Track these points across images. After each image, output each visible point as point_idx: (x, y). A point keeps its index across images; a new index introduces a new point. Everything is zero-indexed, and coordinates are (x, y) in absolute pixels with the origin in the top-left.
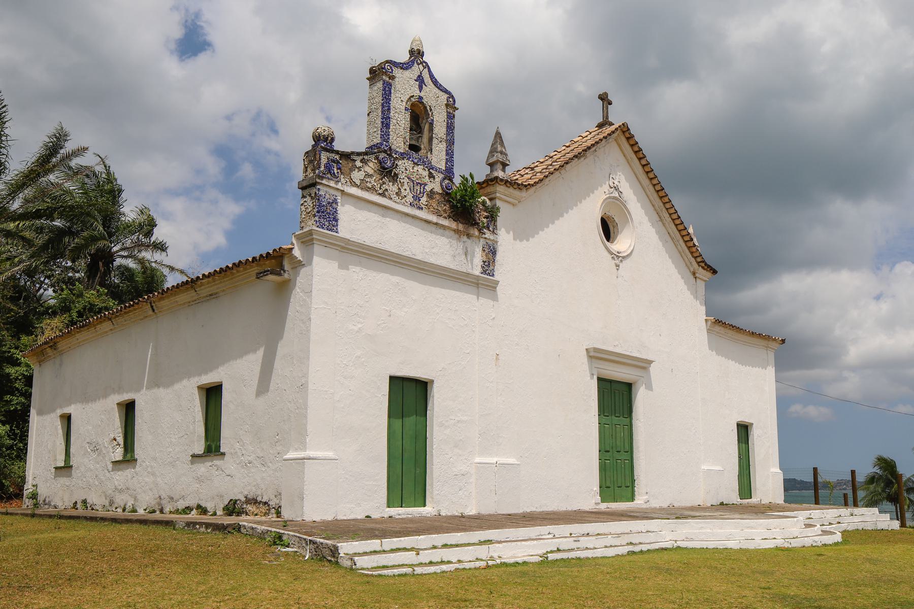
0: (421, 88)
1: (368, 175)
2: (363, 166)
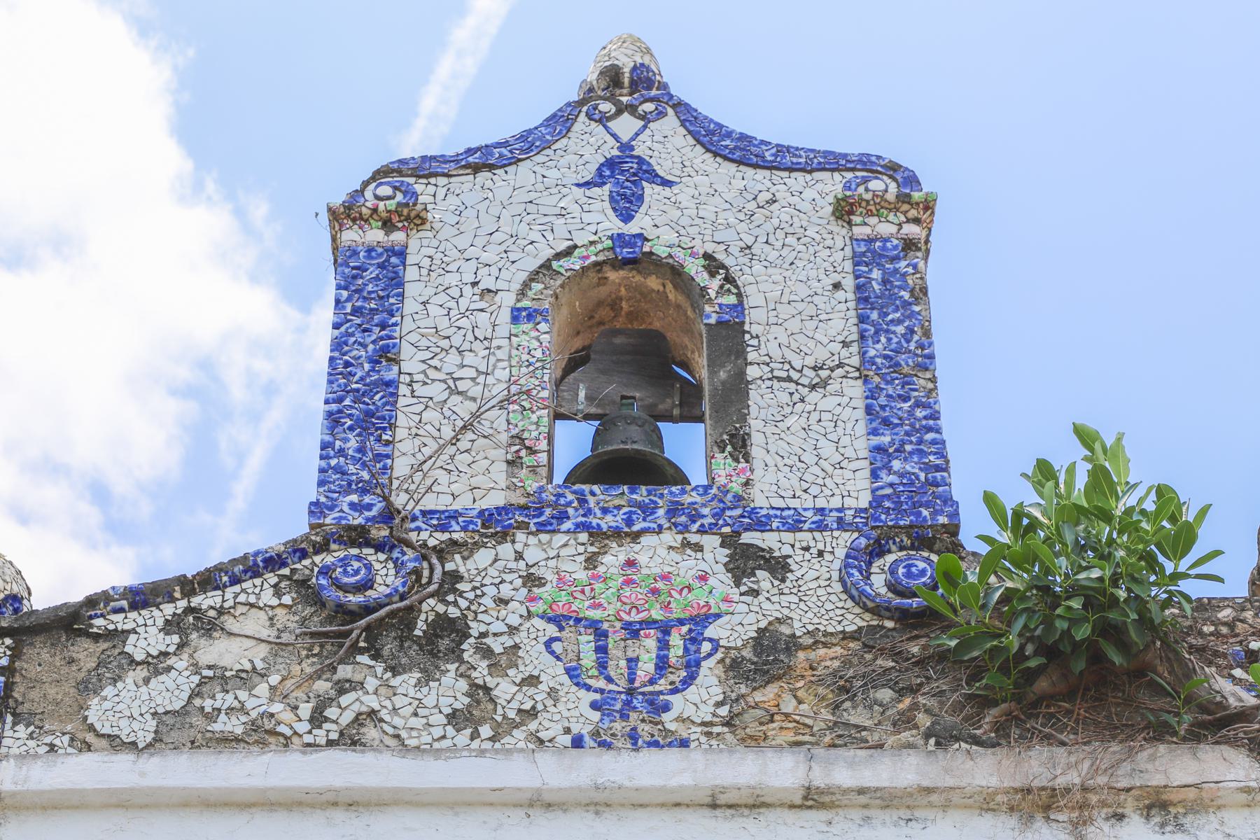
0: (626, 206)
1: (220, 678)
2: (181, 646)
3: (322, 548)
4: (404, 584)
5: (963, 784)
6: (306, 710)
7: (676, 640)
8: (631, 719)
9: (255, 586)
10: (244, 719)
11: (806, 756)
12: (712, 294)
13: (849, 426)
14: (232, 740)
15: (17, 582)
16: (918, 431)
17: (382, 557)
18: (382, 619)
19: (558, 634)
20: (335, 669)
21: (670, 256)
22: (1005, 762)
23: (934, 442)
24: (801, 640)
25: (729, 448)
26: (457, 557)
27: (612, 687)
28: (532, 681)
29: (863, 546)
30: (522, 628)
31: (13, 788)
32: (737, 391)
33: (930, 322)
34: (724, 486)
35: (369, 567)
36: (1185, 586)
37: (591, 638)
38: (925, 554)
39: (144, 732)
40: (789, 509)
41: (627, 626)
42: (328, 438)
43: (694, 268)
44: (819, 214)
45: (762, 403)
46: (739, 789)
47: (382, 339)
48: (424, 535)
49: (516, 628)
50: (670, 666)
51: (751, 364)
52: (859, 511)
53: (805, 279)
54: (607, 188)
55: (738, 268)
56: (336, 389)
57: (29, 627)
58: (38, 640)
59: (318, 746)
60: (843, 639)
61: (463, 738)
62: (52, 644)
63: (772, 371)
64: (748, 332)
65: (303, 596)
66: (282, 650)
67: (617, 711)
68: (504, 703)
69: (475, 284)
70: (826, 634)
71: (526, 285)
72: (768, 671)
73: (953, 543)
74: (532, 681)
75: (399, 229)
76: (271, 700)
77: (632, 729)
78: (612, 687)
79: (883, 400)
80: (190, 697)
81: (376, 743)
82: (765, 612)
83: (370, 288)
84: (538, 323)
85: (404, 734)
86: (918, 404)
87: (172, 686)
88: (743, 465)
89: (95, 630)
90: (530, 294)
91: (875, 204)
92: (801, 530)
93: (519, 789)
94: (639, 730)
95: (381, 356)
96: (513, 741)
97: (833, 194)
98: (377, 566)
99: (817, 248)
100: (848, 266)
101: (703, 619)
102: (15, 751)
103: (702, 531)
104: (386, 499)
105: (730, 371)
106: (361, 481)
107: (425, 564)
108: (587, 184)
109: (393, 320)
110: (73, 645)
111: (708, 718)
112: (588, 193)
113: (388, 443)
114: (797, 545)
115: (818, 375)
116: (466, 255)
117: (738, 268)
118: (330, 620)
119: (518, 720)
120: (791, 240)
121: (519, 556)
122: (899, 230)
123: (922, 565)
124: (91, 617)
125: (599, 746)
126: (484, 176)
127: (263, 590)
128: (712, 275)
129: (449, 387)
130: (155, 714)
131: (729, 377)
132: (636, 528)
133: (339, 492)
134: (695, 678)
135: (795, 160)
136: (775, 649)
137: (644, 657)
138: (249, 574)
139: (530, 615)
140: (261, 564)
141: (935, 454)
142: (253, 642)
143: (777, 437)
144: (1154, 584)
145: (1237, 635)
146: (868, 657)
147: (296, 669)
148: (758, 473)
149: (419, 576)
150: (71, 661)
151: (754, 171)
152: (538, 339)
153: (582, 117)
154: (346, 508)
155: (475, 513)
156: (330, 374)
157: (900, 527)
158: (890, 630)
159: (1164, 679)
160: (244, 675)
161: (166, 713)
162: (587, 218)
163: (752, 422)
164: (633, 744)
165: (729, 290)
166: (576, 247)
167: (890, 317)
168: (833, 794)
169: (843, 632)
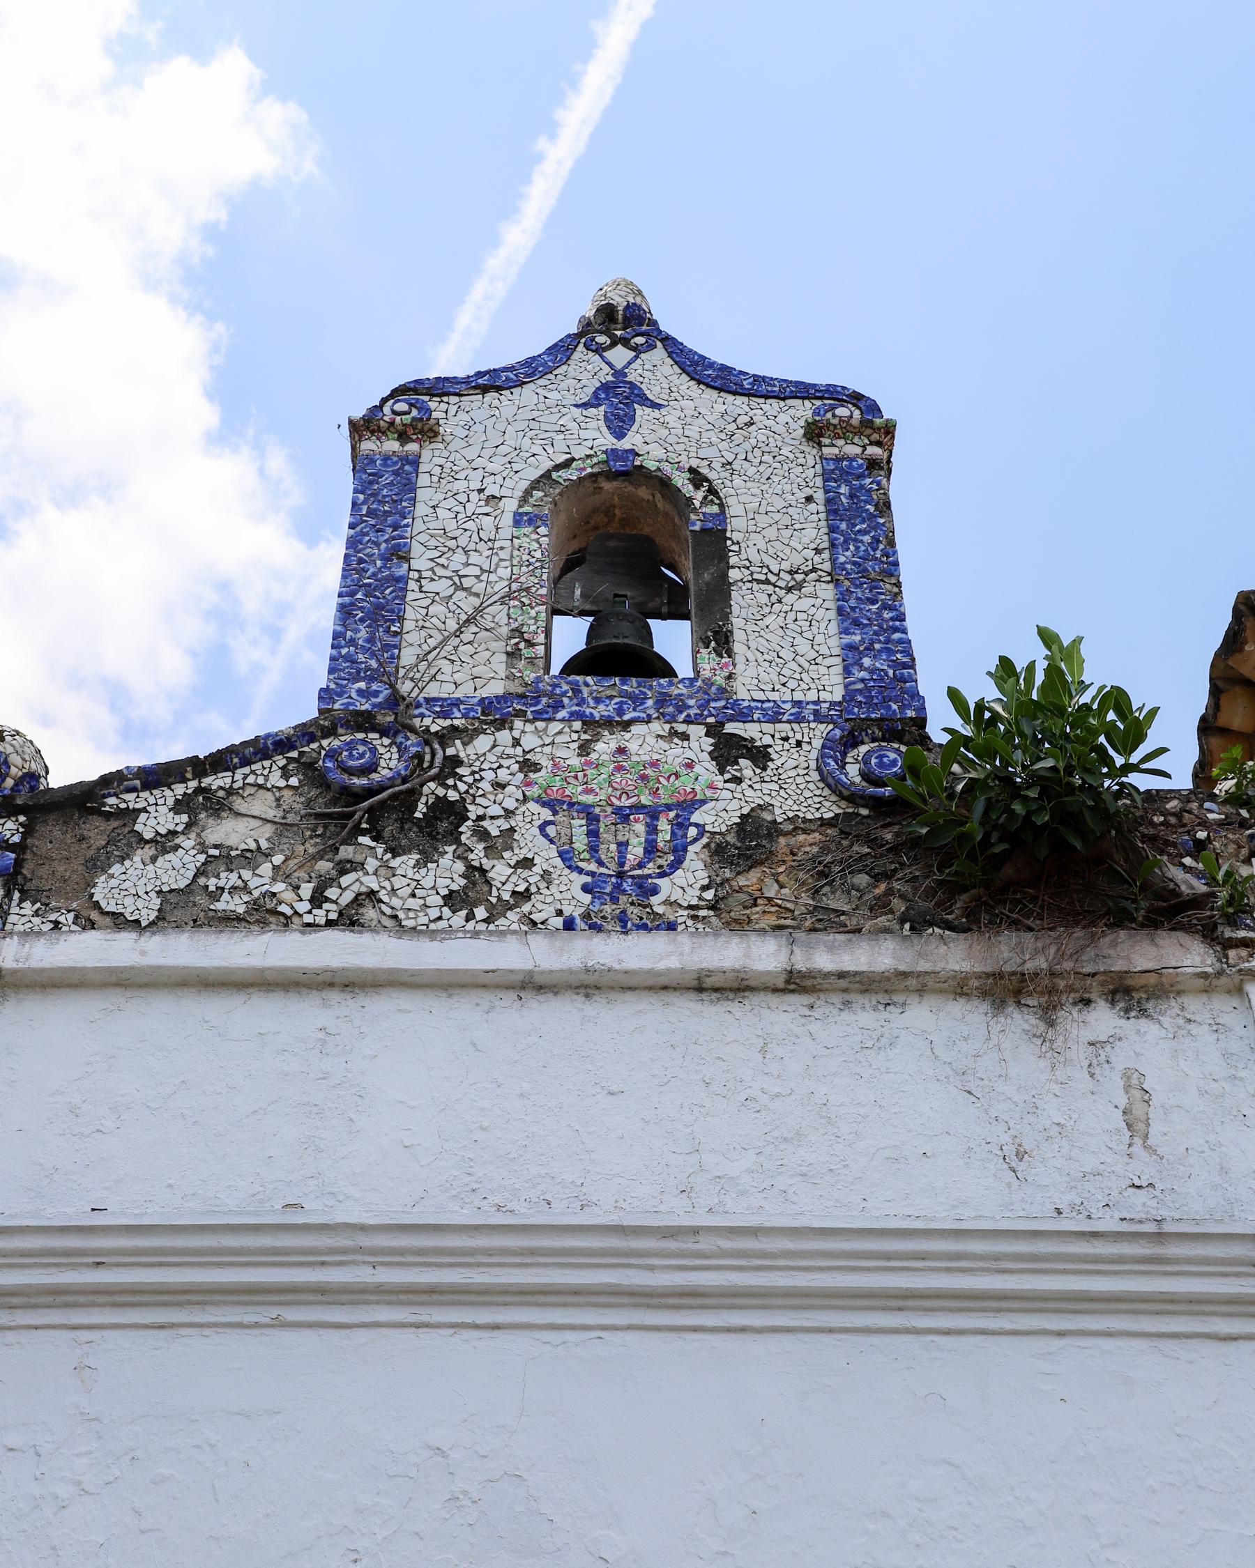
0: (619, 424)
1: (227, 858)
2: (189, 826)
3: (330, 732)
4: (406, 768)
5: (937, 969)
6: (307, 890)
7: (664, 825)
8: (621, 902)
9: (264, 768)
10: (246, 898)
11: (788, 940)
12: (697, 504)
13: (823, 625)
14: (233, 919)
15: (35, 761)
16: (885, 631)
17: (386, 741)
18: (383, 802)
19: (552, 818)
20: (337, 849)
21: (659, 469)
22: (976, 947)
23: (900, 641)
24: (782, 826)
25: (713, 644)
26: (458, 742)
27: (603, 870)
28: (527, 863)
29: (838, 737)
30: (517, 812)
31: (13, 965)
32: (720, 592)
33: (893, 532)
34: (709, 679)
35: (374, 750)
36: (1134, 779)
37: (584, 822)
38: (896, 746)
39: (147, 910)
40: (769, 701)
41: (618, 811)
42: (339, 628)
43: (681, 481)
44: (791, 436)
45: (743, 604)
46: (724, 972)
47: (394, 538)
48: (427, 721)
49: (512, 812)
50: (658, 850)
51: (733, 567)
52: (833, 704)
53: (780, 493)
54: (602, 408)
55: (720, 481)
56: (349, 583)
57: (43, 805)
58: (51, 818)
59: (318, 926)
60: (821, 825)
61: (459, 919)
62: (64, 822)
63: (752, 574)
64: (730, 539)
65: (309, 778)
66: (287, 830)
67: (607, 894)
68: (499, 885)
69: (481, 491)
70: (805, 820)
71: (528, 493)
72: (751, 856)
73: (920, 735)
74: (527, 863)
75: (413, 441)
76: (274, 879)
77: (621, 912)
78: (603, 870)
79: (853, 603)
80: (195, 876)
81: (374, 923)
82: (748, 799)
83: (385, 492)
84: (539, 527)
85: (401, 915)
86: (885, 607)
87: (178, 864)
88: (726, 660)
89: (107, 809)
90: (531, 500)
91: (842, 428)
92: (780, 722)
93: (512, 971)
94: (629, 912)
95: (392, 554)
96: (507, 923)
97: (804, 418)
98: (382, 750)
99: (791, 465)
100: (819, 481)
101: (690, 804)
102: (19, 928)
103: (688, 721)
104: (392, 686)
105: (713, 574)
106: (370, 669)
107: (427, 749)
108: (585, 405)
109: (405, 522)
110: (84, 823)
111: (695, 902)
112: (585, 413)
113: (396, 634)
114: (777, 736)
115: (793, 579)
116: (474, 465)
117: (720, 481)
118: (334, 802)
119: (512, 902)
120: (767, 458)
121: (516, 742)
122: (864, 451)
123: (892, 756)
124: (104, 796)
125: (590, 929)
126: (491, 396)
127: (272, 772)
128: (697, 487)
129: (455, 583)
130: (159, 893)
131: (713, 578)
132: (626, 717)
133: (348, 680)
134: (682, 862)
135: (770, 389)
136: (758, 834)
137: (634, 841)
138: (259, 756)
139: (525, 799)
140: (271, 747)
141: (902, 652)
142: (259, 823)
143: (757, 634)
144: (1107, 775)
145: (1184, 825)
146: (845, 843)
147: (300, 849)
148: (740, 667)
149: (421, 759)
150: (82, 839)
151: (733, 397)
152: (537, 541)
153: (581, 347)
154: (354, 695)
155: (476, 700)
156: (344, 570)
157: (872, 720)
158: (864, 817)
159: (1121, 866)
160: (248, 855)
161: (172, 891)
162: (584, 434)
163: (734, 621)
164: (622, 927)
165: (712, 501)
166: (573, 459)
167: (858, 528)
168: (815, 978)
169: (821, 818)
